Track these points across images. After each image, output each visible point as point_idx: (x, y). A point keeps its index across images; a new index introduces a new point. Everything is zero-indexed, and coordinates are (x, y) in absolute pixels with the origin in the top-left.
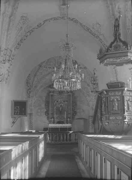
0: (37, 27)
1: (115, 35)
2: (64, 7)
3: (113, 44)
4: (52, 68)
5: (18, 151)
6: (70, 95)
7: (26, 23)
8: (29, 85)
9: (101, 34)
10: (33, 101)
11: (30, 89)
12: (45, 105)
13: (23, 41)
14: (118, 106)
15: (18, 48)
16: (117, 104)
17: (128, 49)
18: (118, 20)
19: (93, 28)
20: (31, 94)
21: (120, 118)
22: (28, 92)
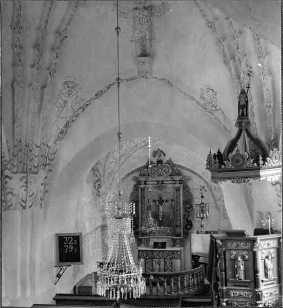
1: (239, 124)
2: (143, 59)
3: (230, 154)
5: (105, 248)
7: (75, 92)
9: (219, 110)
13: (69, 124)
14: (245, 271)
15: (60, 138)
16: (242, 268)
17: (258, 164)
18: (245, 92)
19: (202, 97)
20: (102, 190)
21: (248, 295)
22: (97, 187)
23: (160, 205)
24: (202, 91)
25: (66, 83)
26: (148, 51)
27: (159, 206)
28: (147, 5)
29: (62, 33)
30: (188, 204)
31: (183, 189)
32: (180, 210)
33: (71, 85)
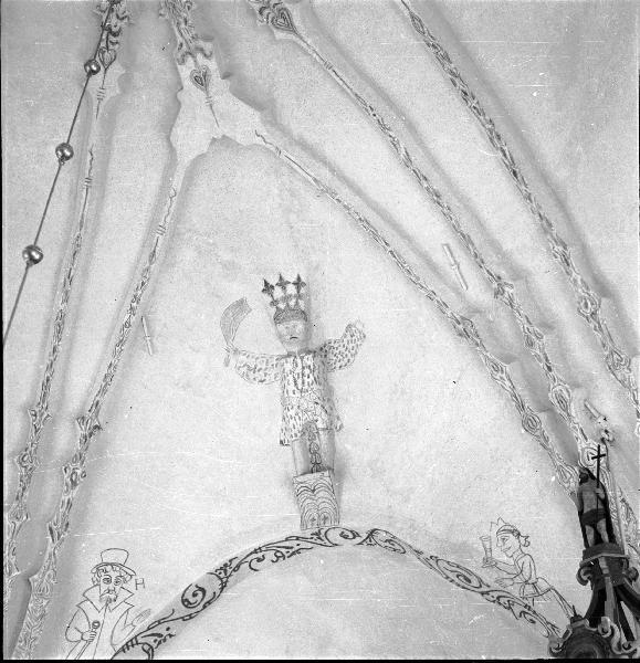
0: (185, 611)
2: (311, 478)
7: (123, 595)
18: (593, 477)
19: (489, 562)
24: (488, 545)
25: (100, 568)
26: (326, 460)
28: (315, 343)
29: (88, 415)
33: (114, 575)
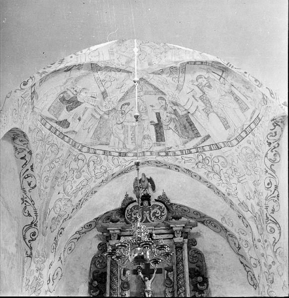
4: (113, 154)
6: (179, 247)
8: (30, 209)
10: (45, 273)
11: (33, 224)
12: (90, 284)
22: (28, 238)
23: (147, 278)
27: (144, 282)
30: (199, 275)
31: (189, 248)
32: (184, 286)
